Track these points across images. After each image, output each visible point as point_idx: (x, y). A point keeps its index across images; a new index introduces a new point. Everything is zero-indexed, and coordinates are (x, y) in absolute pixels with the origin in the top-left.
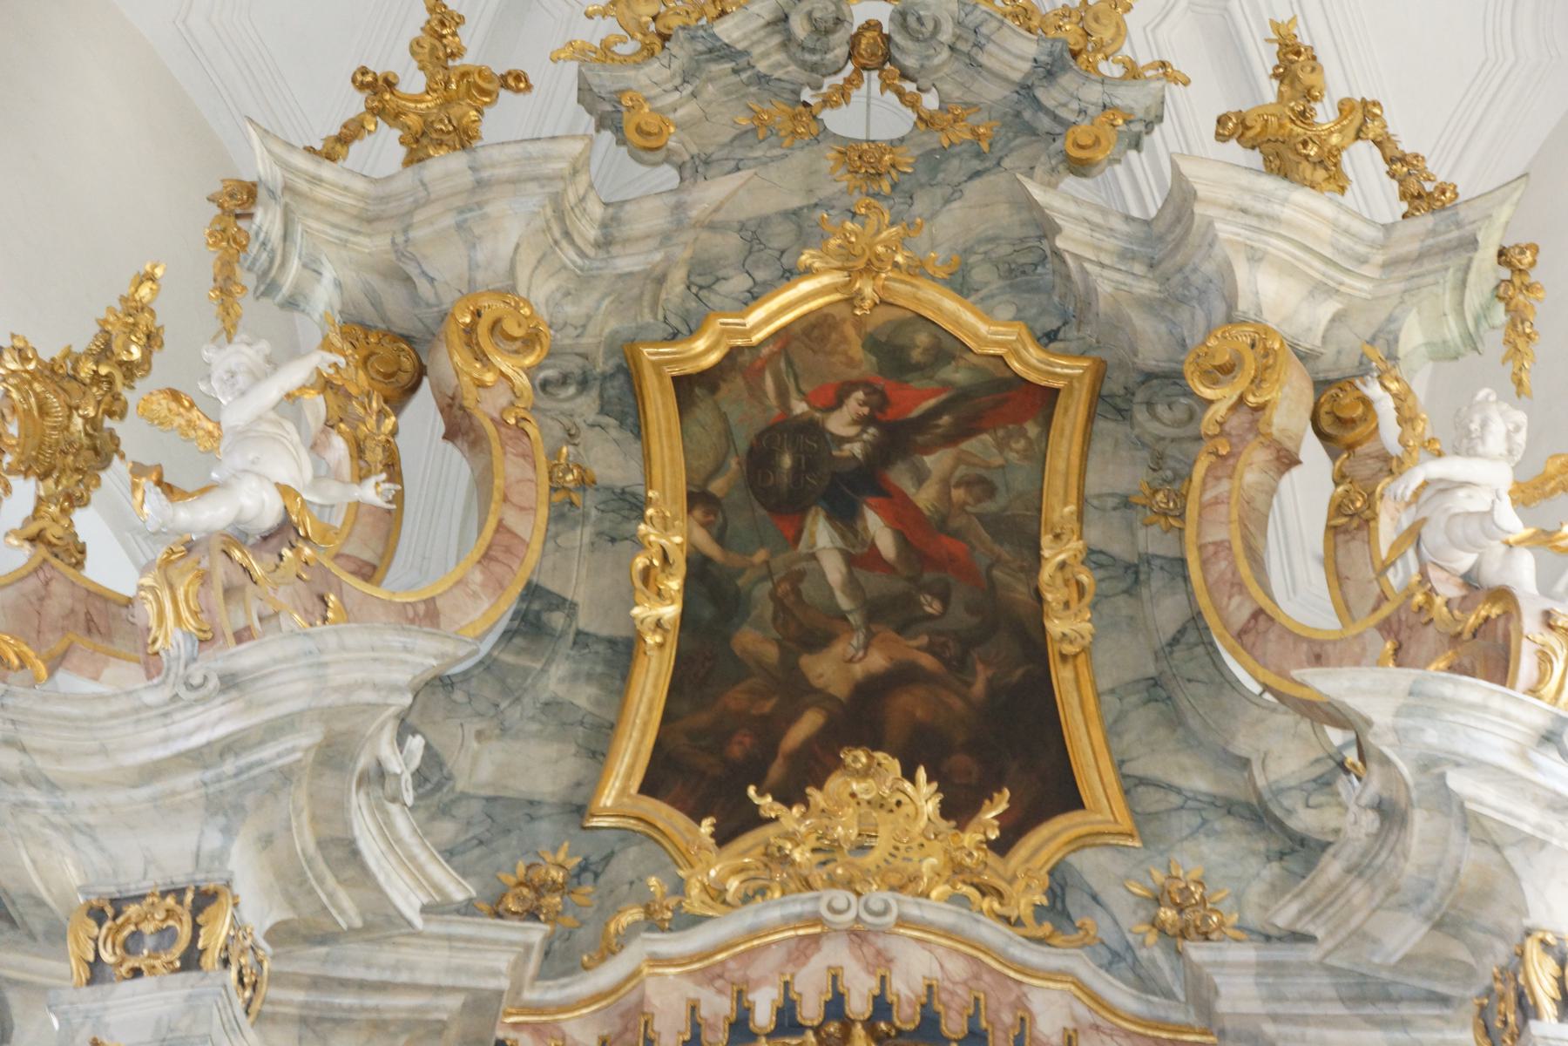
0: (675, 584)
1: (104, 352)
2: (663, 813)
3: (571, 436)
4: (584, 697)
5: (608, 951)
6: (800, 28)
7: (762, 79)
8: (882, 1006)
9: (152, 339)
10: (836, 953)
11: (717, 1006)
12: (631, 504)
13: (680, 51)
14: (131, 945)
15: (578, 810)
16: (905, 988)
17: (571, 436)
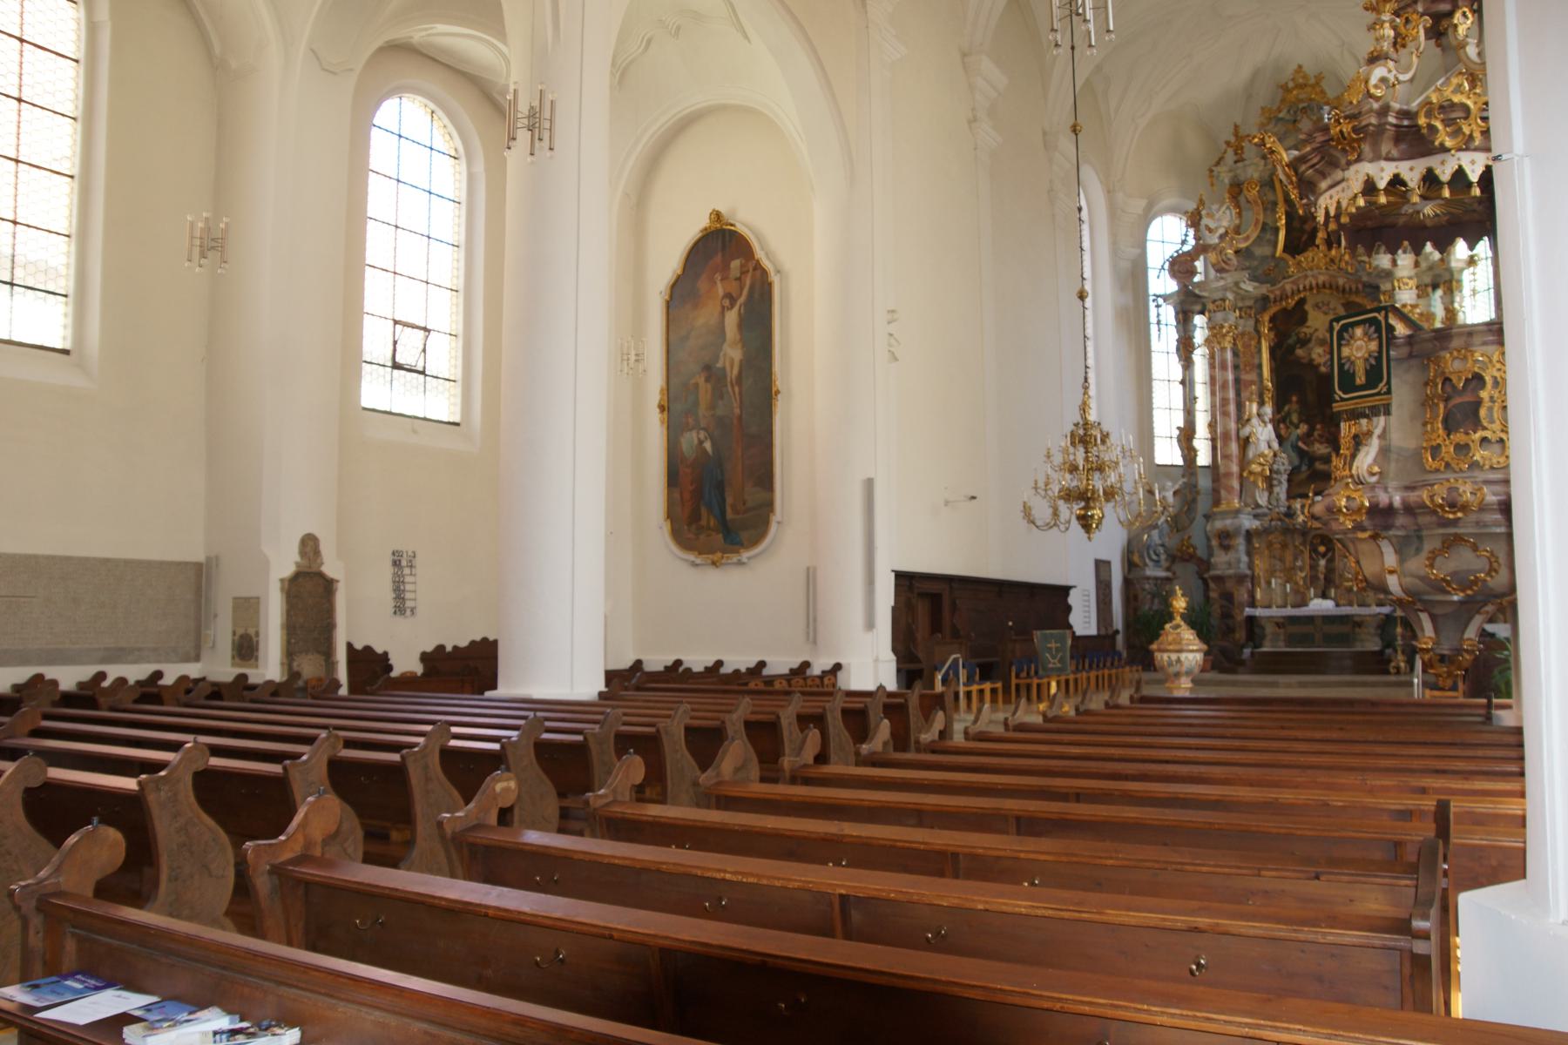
0: (1284, 217)
1: (1198, 208)
2: (1287, 256)
3: (1265, 195)
4: (1272, 238)
5: (1279, 282)
6: (1292, 112)
7: (1288, 121)
8: (1317, 284)
9: (1203, 205)
10: (1310, 279)
11: (1295, 288)
12: (1275, 204)
13: (1273, 122)
14: (1217, 307)
15: (1273, 256)
16: (1320, 282)
17: (1265, 195)
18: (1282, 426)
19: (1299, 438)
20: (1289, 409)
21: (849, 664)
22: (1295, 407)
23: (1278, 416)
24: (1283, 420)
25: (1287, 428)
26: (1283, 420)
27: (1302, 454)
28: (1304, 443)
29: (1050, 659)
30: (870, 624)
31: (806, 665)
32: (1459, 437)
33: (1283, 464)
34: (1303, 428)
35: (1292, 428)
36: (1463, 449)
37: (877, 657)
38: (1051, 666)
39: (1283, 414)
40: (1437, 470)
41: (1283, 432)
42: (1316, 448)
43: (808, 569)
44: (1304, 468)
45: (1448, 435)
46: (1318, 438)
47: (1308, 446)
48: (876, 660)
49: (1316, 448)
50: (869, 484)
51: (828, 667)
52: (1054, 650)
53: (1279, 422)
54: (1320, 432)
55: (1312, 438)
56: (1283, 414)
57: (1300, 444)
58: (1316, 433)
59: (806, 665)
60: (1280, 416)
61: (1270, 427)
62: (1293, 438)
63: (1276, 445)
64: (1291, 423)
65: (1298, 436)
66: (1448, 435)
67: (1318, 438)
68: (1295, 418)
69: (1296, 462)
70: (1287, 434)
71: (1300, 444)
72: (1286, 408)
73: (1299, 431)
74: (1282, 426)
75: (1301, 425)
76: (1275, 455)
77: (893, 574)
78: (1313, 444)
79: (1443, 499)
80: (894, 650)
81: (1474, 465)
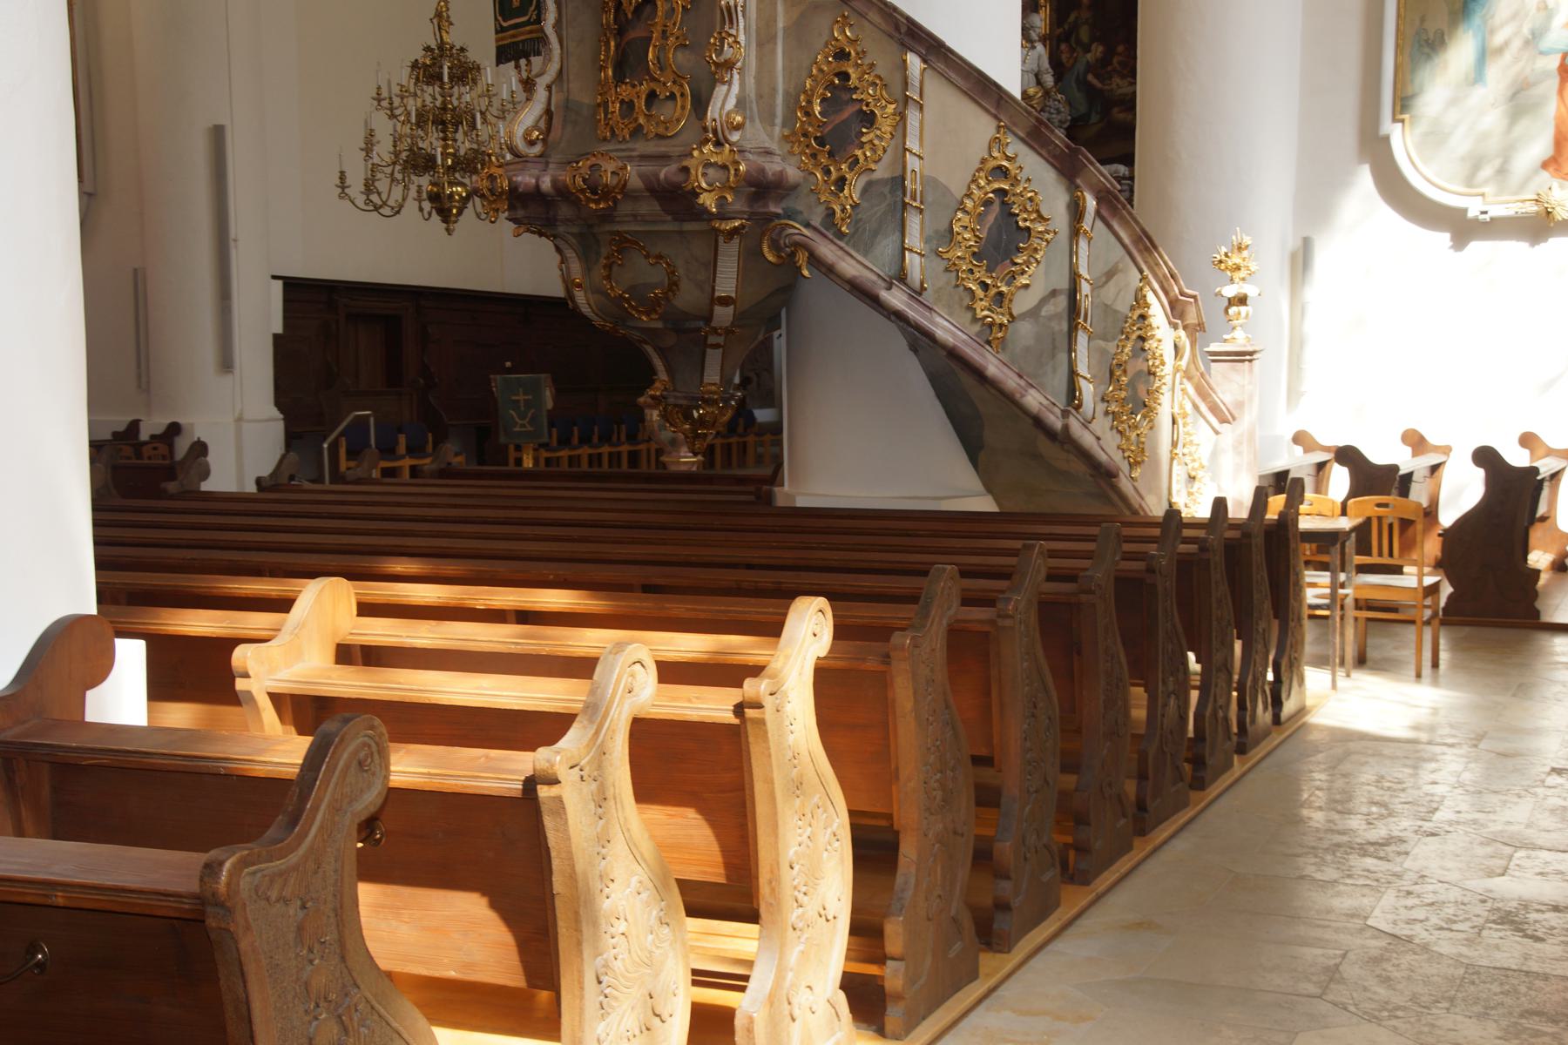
18: (1063, 46)
19: (1089, 68)
20: (1077, 18)
21: (192, 425)
22: (1085, 14)
23: (1059, 31)
24: (1066, 37)
25: (1072, 50)
26: (1066, 37)
27: (1091, 93)
28: (1097, 76)
29: (517, 420)
30: (226, 364)
31: (134, 426)
32: (625, 91)
33: (1059, 112)
34: (1098, 50)
35: (1079, 49)
36: (628, 106)
37: (241, 414)
38: (517, 429)
39: (1066, 27)
40: (605, 139)
41: (1064, 57)
42: (1114, 86)
43: (135, 271)
44: (1094, 118)
45: (616, 87)
46: (1118, 68)
47: (1102, 82)
48: (239, 420)
49: (1114, 86)
50: (218, 135)
51: (159, 431)
52: (522, 404)
53: (1059, 40)
54: (1121, 58)
55: (1109, 68)
56: (1066, 27)
57: (1090, 77)
58: (1115, 60)
59: (134, 426)
60: (1061, 30)
61: (1040, 47)
62: (1080, 67)
63: (1049, 80)
64: (1079, 42)
65: (1088, 62)
66: (616, 87)
67: (1118, 68)
68: (1084, 34)
69: (1083, 109)
70: (1071, 61)
71: (1090, 77)
72: (1072, 18)
73: (1089, 56)
74: (1063, 46)
75: (1094, 46)
76: (1047, 93)
77: (280, 283)
78: (1111, 78)
79: (584, 180)
80: (279, 403)
81: (637, 132)
